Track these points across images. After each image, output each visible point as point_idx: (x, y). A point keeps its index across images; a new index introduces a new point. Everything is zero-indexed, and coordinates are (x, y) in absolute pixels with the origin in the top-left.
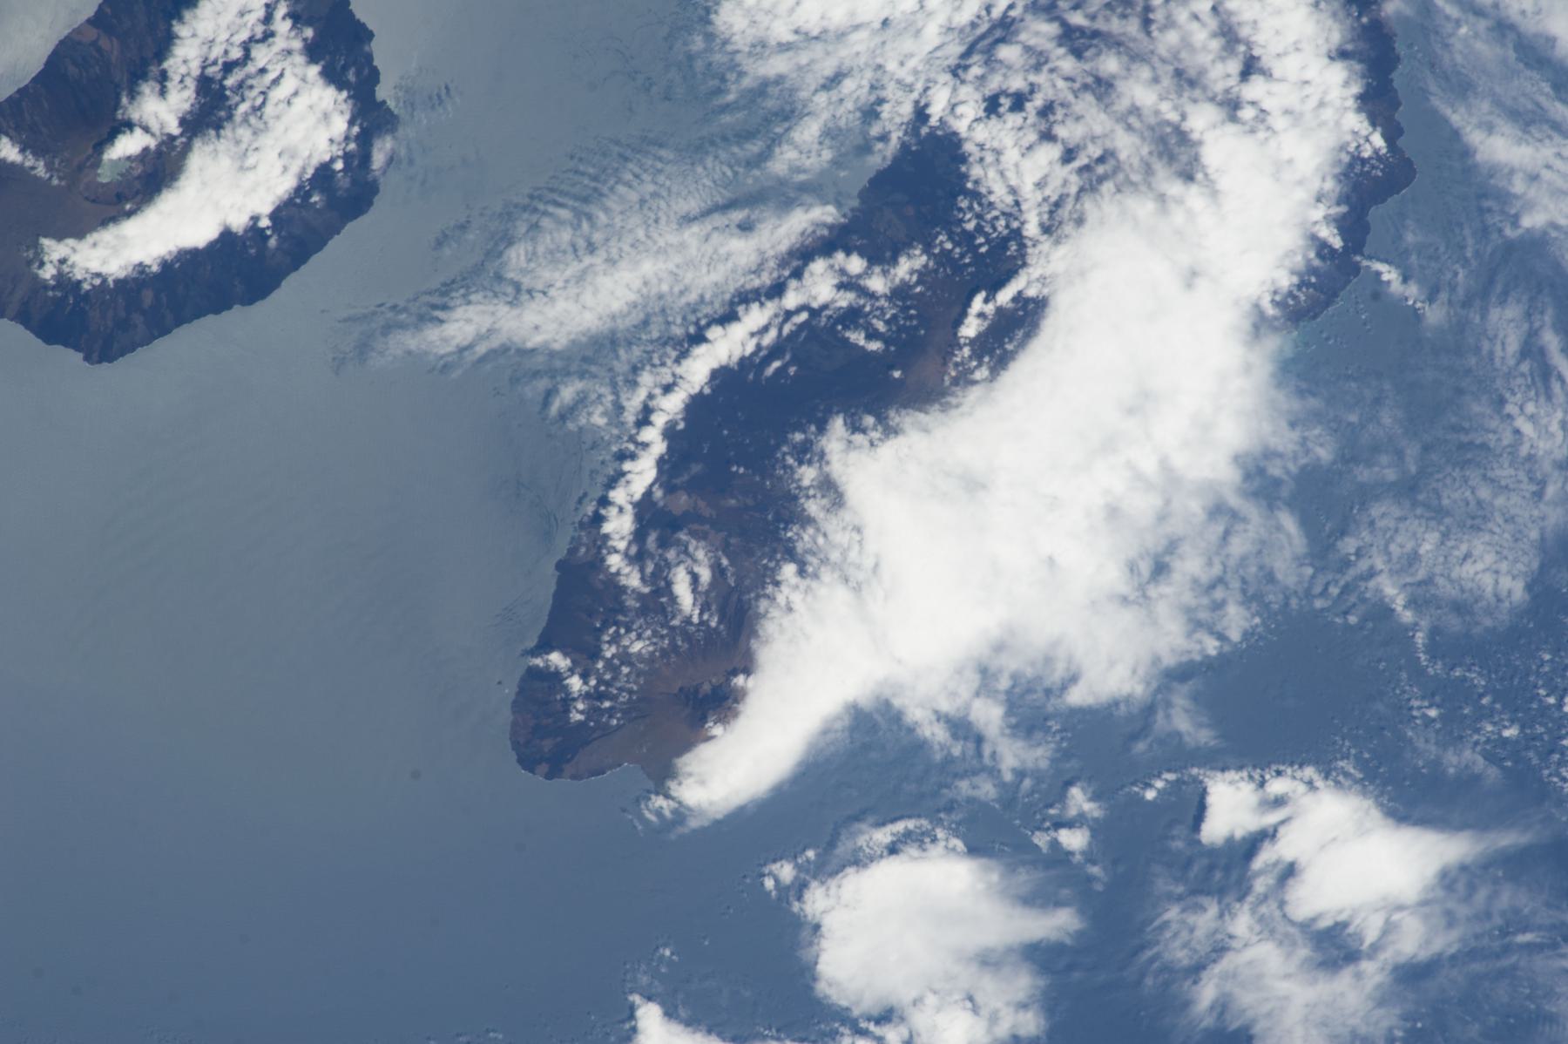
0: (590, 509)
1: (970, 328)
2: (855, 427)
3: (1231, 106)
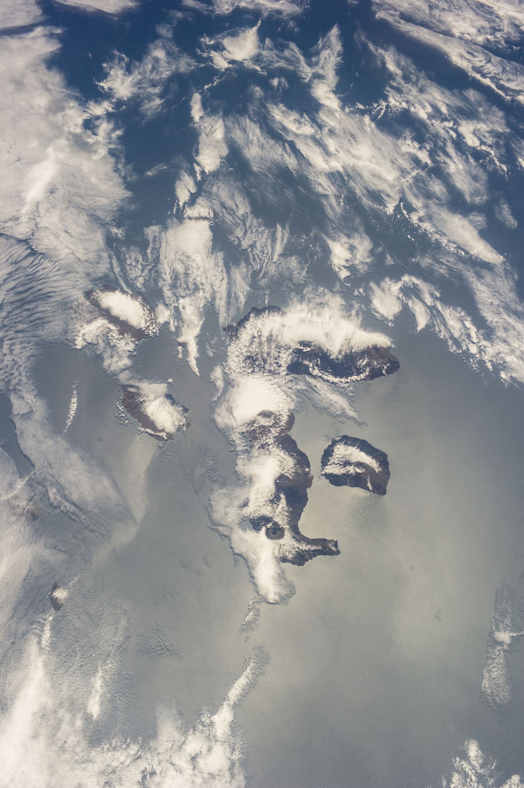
0: (363, 381)
1: (308, 349)
2: (330, 355)
3: (260, 336)
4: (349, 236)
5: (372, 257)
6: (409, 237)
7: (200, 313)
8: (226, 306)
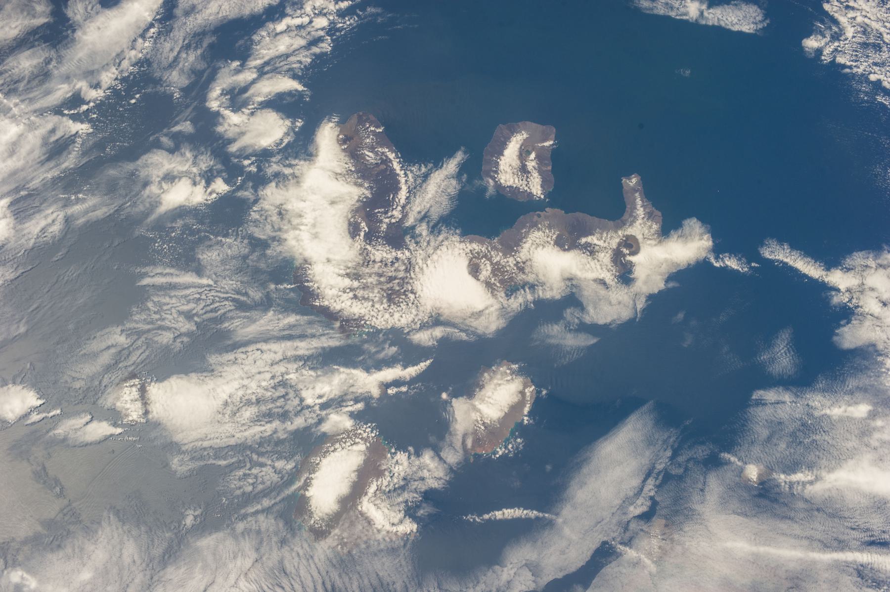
1: (363, 224)
3: (351, 290)
4: (146, 184)
5: (183, 150)
6: (133, 101)
7: (325, 374)
8: (308, 340)
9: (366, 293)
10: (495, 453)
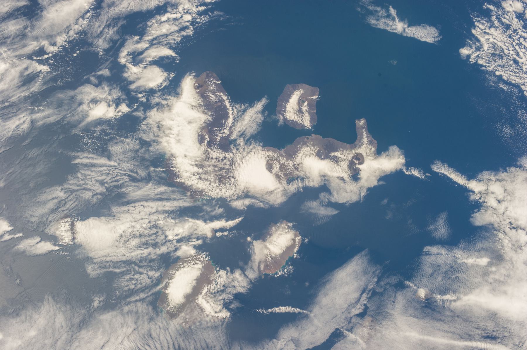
1: (207, 136)
2: (209, 121)
3: (198, 174)
4: (80, 104)
5: (103, 86)
6: (75, 55)
7: (180, 222)
8: (172, 202)
9: (206, 176)
10: (277, 274)
